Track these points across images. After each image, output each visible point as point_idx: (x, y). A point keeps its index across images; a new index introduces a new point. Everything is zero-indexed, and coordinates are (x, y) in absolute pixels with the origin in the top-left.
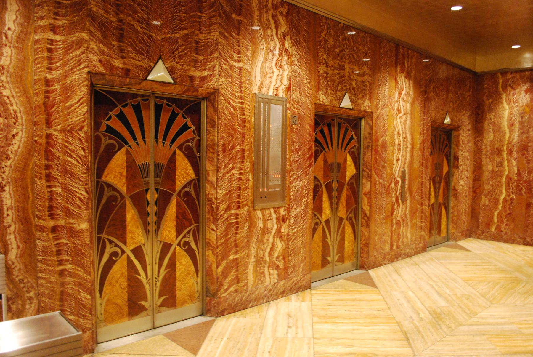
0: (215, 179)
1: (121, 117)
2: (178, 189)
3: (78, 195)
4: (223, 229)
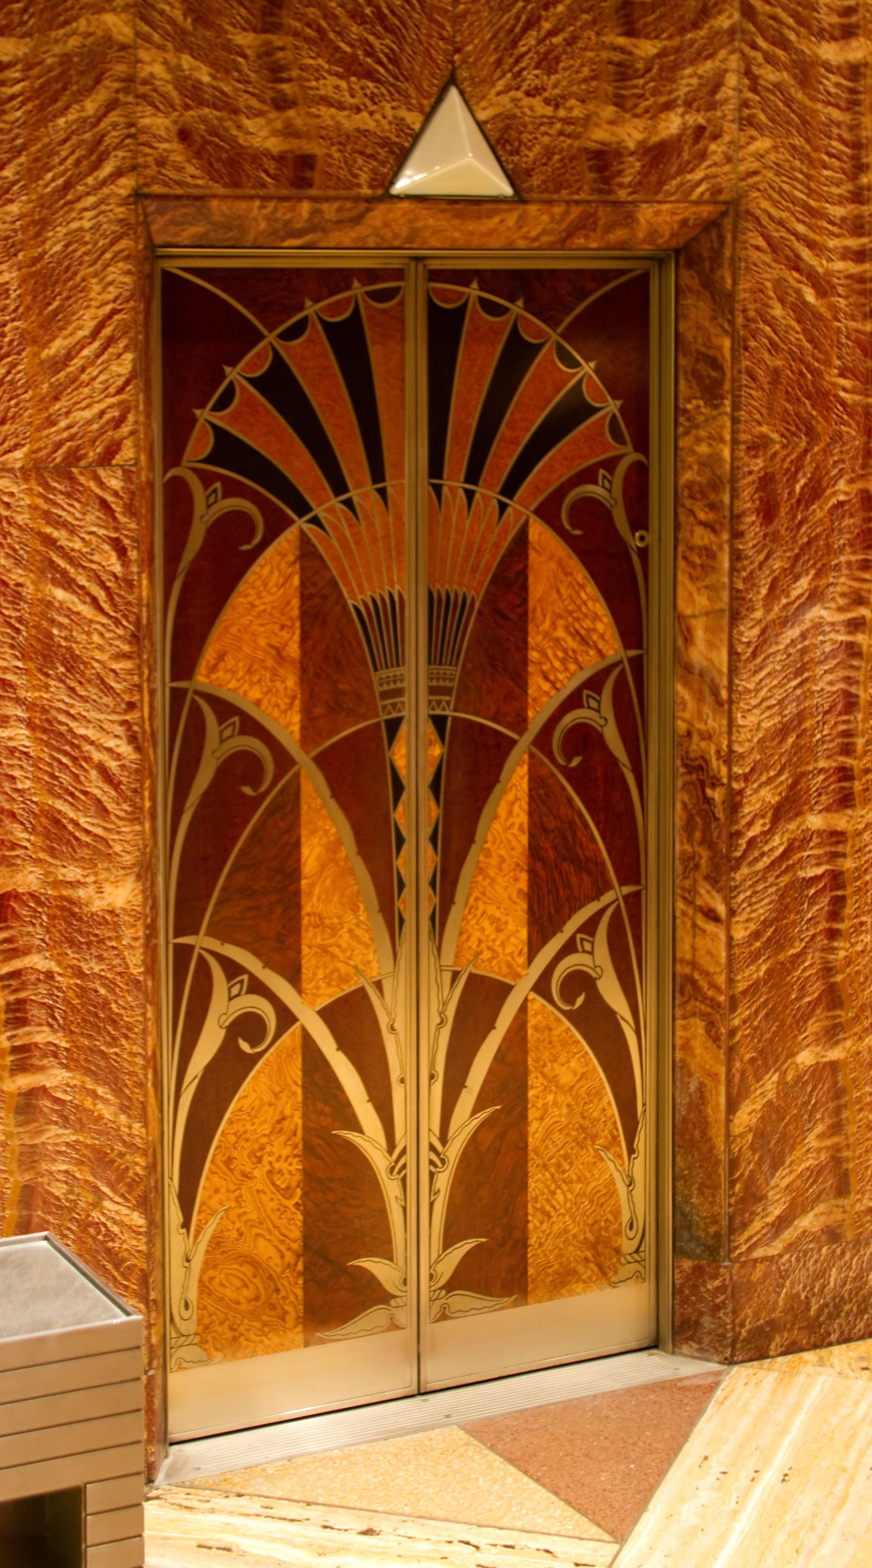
0: (722, 658)
2: (536, 718)
3: (97, 756)
4: (762, 911)
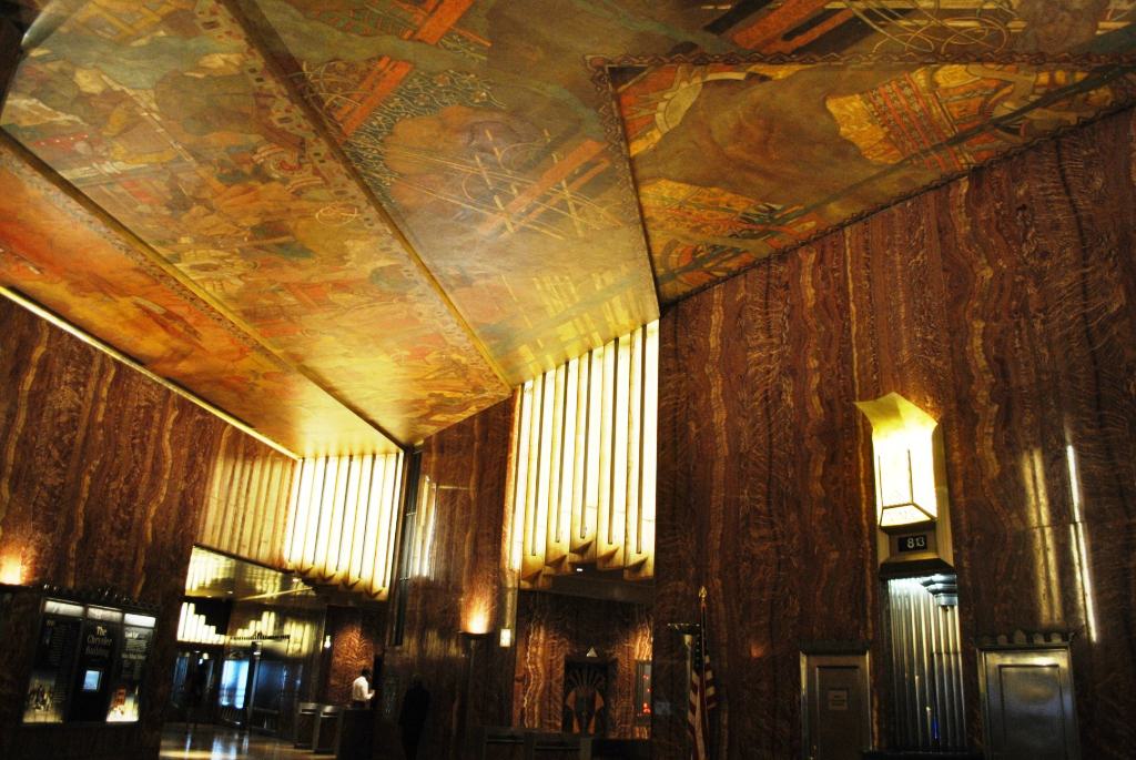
1: (575, 676)
